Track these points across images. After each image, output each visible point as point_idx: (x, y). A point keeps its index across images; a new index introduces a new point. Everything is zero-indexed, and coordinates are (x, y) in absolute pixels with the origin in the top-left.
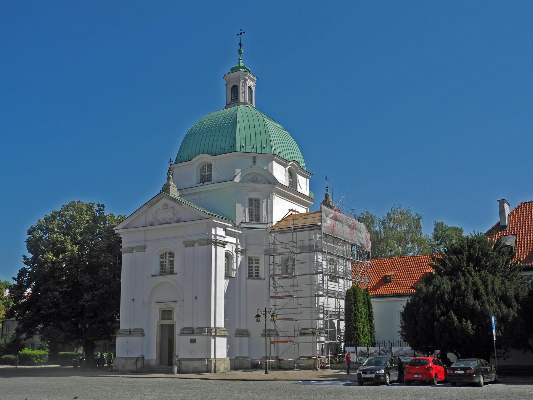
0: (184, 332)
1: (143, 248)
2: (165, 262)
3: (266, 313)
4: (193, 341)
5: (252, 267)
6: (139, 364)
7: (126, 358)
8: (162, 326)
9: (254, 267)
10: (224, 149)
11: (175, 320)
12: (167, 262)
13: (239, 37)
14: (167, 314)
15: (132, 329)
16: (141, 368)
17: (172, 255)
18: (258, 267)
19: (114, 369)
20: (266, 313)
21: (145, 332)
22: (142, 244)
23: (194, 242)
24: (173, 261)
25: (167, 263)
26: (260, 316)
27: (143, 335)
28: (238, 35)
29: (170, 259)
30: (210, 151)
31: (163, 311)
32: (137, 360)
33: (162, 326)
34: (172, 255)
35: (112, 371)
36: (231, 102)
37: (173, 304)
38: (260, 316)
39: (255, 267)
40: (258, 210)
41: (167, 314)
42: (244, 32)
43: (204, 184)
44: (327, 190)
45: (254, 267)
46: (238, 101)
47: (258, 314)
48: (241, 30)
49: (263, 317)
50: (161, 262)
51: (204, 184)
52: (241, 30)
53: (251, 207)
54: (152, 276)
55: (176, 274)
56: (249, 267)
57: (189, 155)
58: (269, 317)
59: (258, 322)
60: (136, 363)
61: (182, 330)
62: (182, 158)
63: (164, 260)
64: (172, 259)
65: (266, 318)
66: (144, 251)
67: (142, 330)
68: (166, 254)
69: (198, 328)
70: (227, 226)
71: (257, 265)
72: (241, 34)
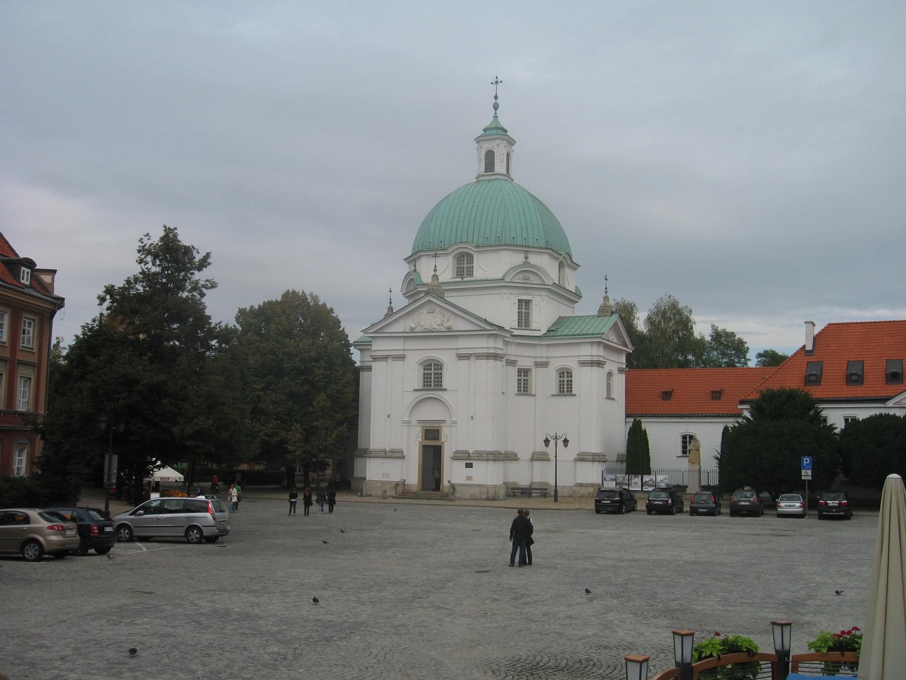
0: (458, 456)
1: (402, 358)
2: (431, 374)
3: (556, 437)
4: (469, 466)
5: (520, 380)
6: (400, 489)
7: (382, 483)
8: (424, 446)
9: (522, 380)
10: (489, 239)
11: (443, 439)
12: (432, 374)
13: (494, 86)
14: (432, 433)
15: (387, 450)
16: (403, 493)
17: (439, 367)
18: (527, 380)
19: (364, 493)
20: (556, 437)
21: (405, 454)
22: (401, 353)
23: (471, 354)
24: (441, 374)
25: (432, 376)
26: (549, 441)
27: (403, 457)
28: (492, 83)
29: (437, 371)
30: (470, 239)
31: (426, 431)
32: (397, 484)
33: (425, 448)
34: (439, 366)
35: (361, 496)
36: (485, 172)
37: (441, 425)
38: (549, 441)
39: (524, 380)
40: (528, 313)
41: (432, 433)
42: (501, 82)
43: (462, 279)
44: (606, 292)
45: (522, 380)
46: (496, 172)
47: (547, 439)
48: (497, 78)
49: (552, 443)
50: (424, 374)
51: (462, 279)
52: (497, 78)
53: (520, 310)
54: (415, 390)
55: (446, 390)
56: (518, 379)
57: (441, 241)
58: (560, 443)
59: (547, 445)
60: (396, 487)
61: (454, 453)
62: (432, 243)
63: (429, 372)
64: (439, 371)
65: (556, 443)
66: (404, 361)
67: (402, 452)
68: (431, 365)
69: (477, 452)
70: (506, 337)
71: (526, 378)
72: (497, 82)
